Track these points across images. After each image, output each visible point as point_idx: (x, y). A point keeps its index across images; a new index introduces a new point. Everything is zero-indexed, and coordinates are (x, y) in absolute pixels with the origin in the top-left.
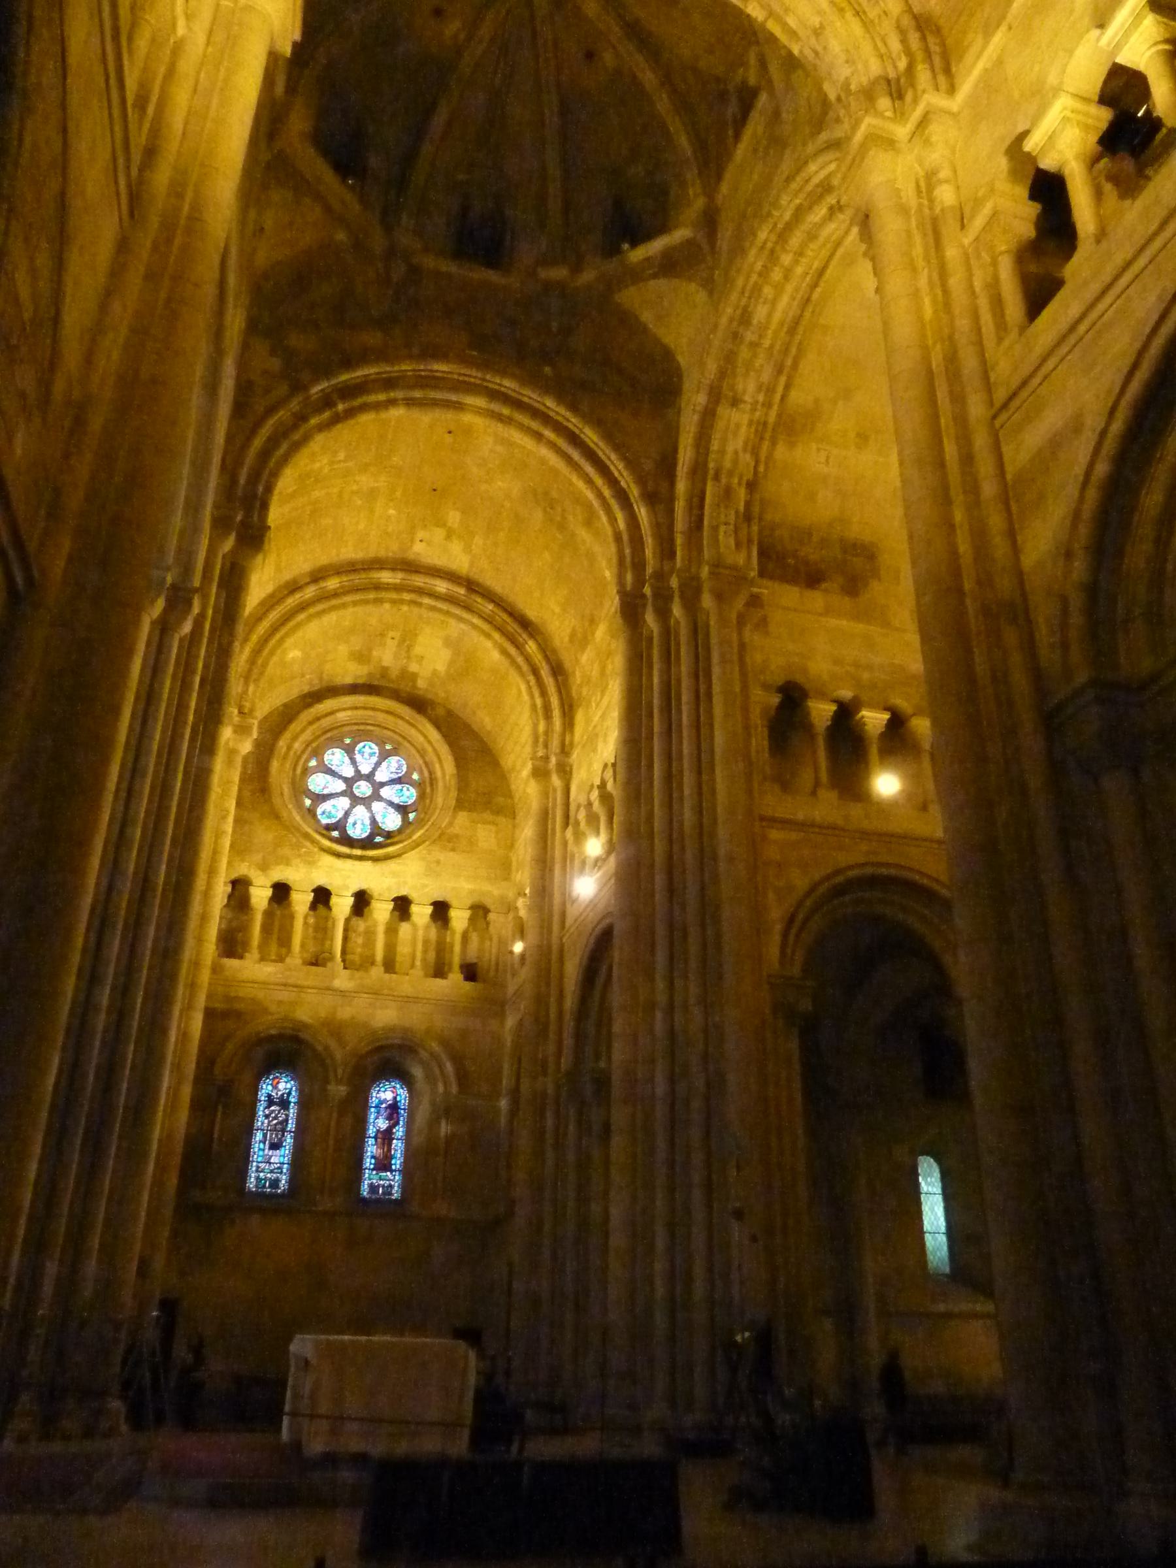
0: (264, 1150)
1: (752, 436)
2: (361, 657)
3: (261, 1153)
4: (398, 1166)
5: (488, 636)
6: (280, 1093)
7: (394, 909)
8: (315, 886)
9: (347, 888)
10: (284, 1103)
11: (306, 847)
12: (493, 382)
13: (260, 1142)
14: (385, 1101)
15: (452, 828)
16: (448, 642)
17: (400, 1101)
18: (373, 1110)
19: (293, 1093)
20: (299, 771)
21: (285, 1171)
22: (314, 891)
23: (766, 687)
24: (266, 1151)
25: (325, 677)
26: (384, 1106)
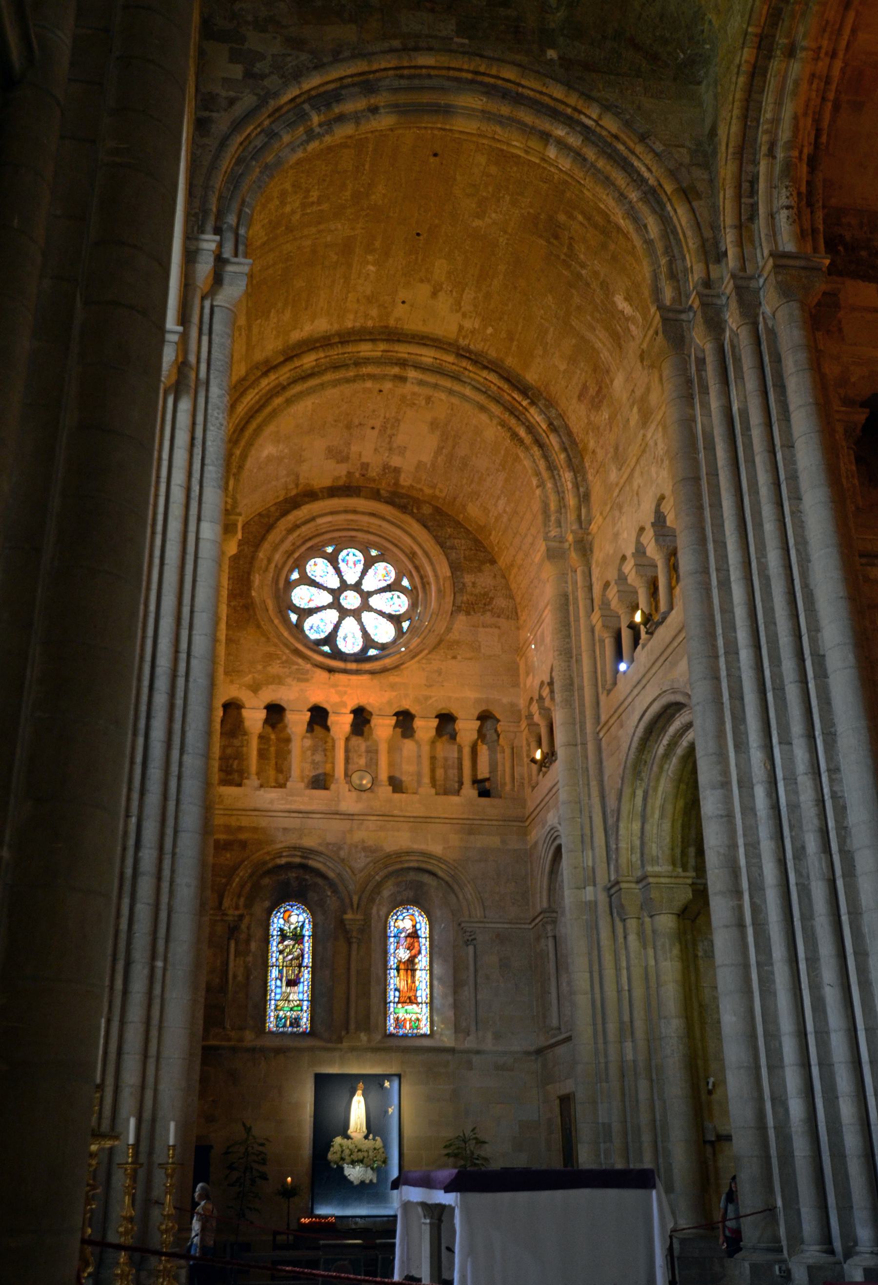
0: (281, 987)
1: (814, 94)
2: (338, 455)
3: (278, 991)
4: (424, 999)
5: (483, 408)
6: (292, 927)
7: (396, 726)
8: (310, 706)
9: (344, 705)
10: (298, 938)
11: (298, 664)
12: (489, 75)
14: (404, 930)
15: (450, 635)
16: (434, 425)
18: (392, 940)
19: (307, 926)
20: (281, 584)
21: (305, 1008)
22: (310, 710)
23: (848, 402)
24: (284, 988)
25: (302, 480)
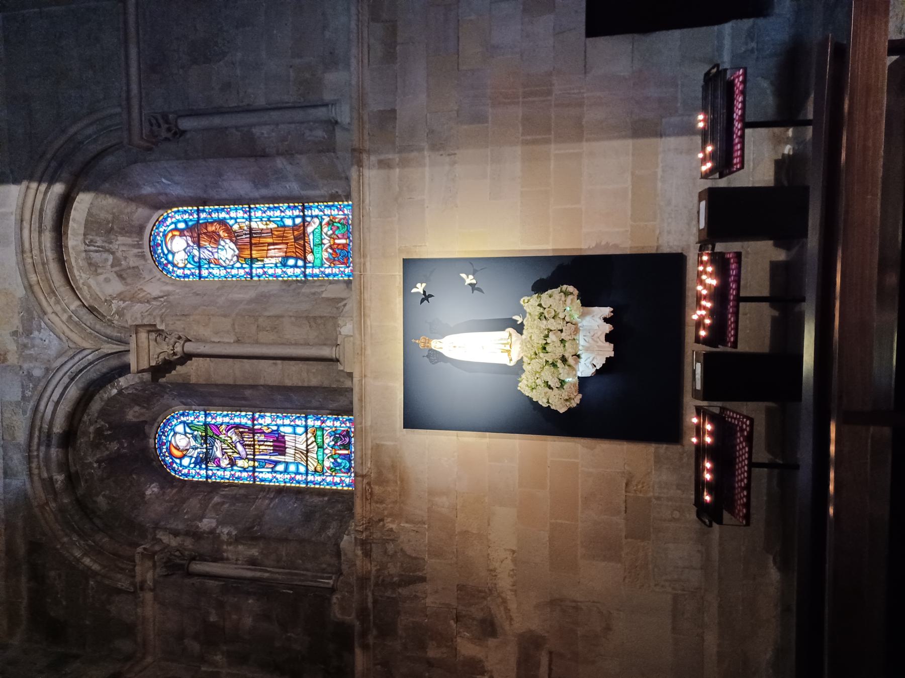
0: (287, 464)
3: (292, 468)
4: (296, 213)
6: (193, 443)
10: (209, 435)
13: (273, 471)
17: (186, 222)
21: (318, 423)
24: (288, 459)
26: (196, 252)
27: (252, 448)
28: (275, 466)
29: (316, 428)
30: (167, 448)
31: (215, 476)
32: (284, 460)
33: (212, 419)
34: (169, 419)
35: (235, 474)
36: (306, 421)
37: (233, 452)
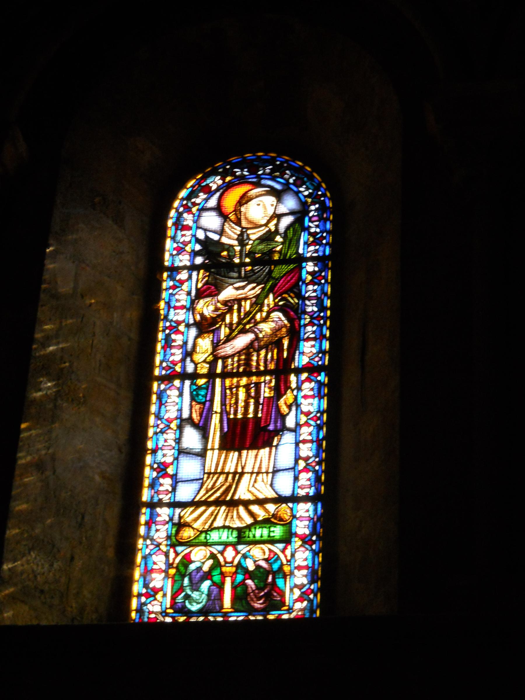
0: (202, 454)
6: (255, 234)
24: (212, 457)
27: (241, 370)
28: (195, 426)
29: (290, 523)
30: (243, 177)
31: (174, 287)
32: (209, 446)
33: (312, 274)
34: (311, 178)
35: (178, 332)
36: (306, 499)
37: (231, 324)
